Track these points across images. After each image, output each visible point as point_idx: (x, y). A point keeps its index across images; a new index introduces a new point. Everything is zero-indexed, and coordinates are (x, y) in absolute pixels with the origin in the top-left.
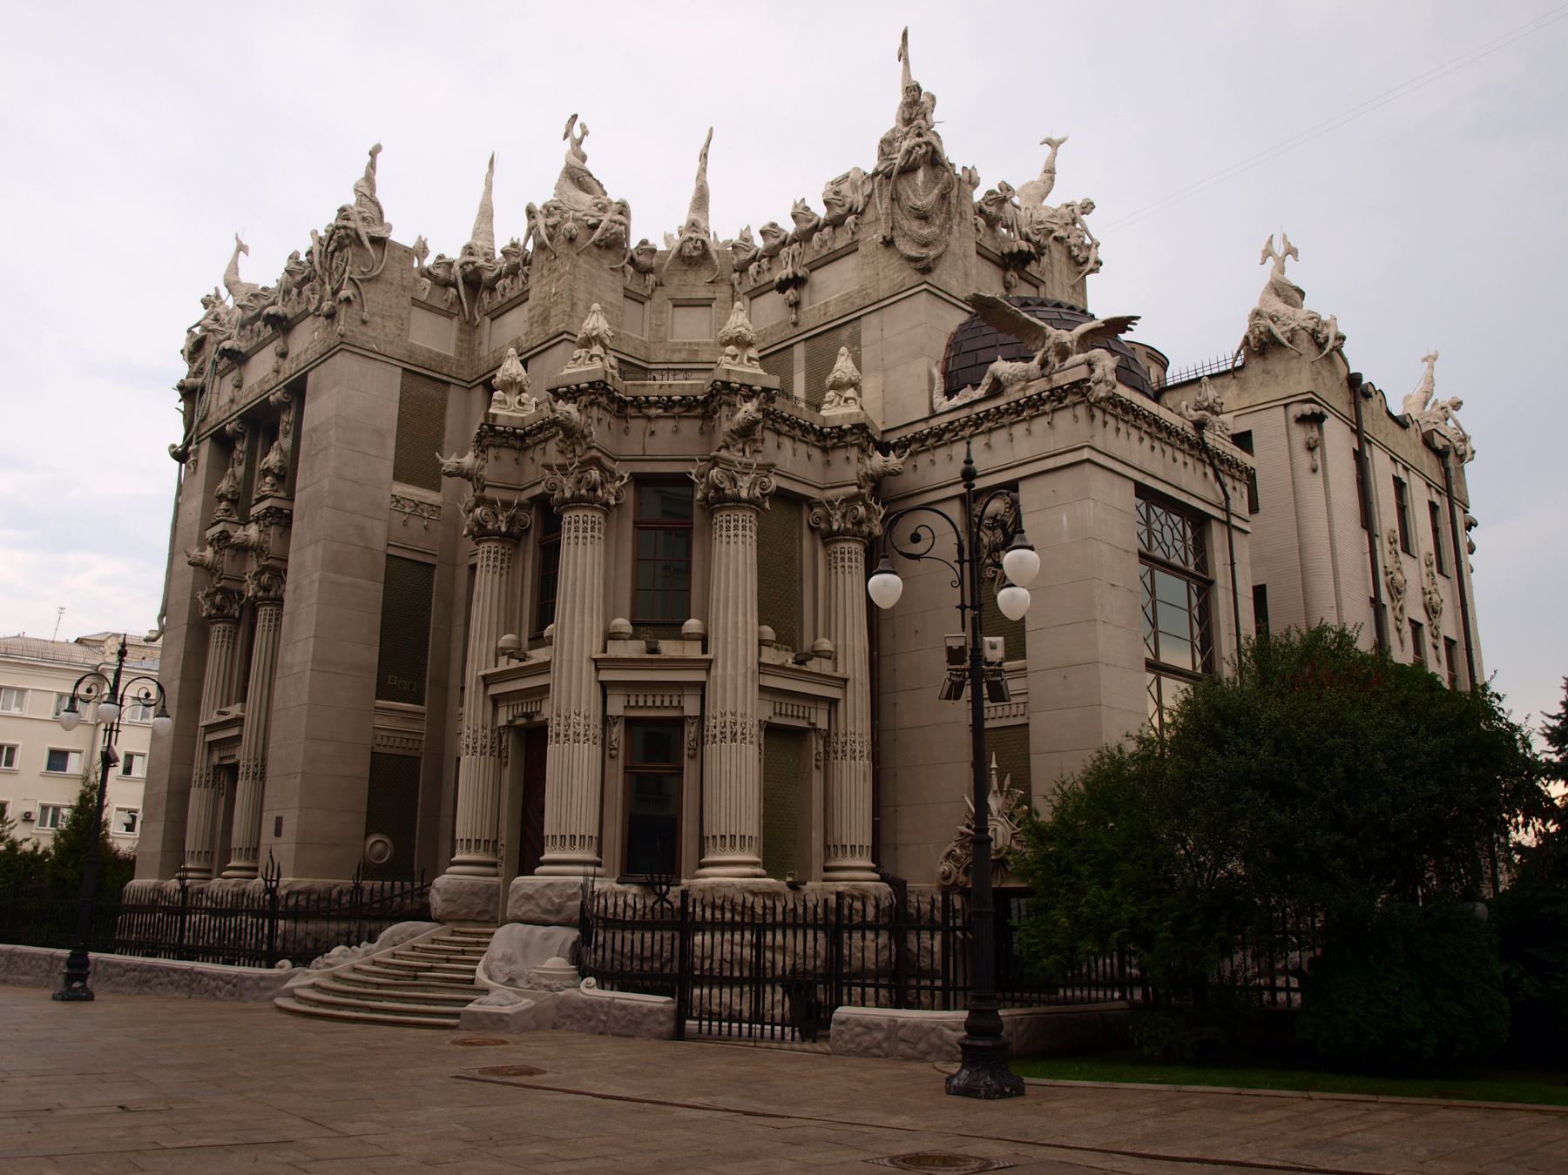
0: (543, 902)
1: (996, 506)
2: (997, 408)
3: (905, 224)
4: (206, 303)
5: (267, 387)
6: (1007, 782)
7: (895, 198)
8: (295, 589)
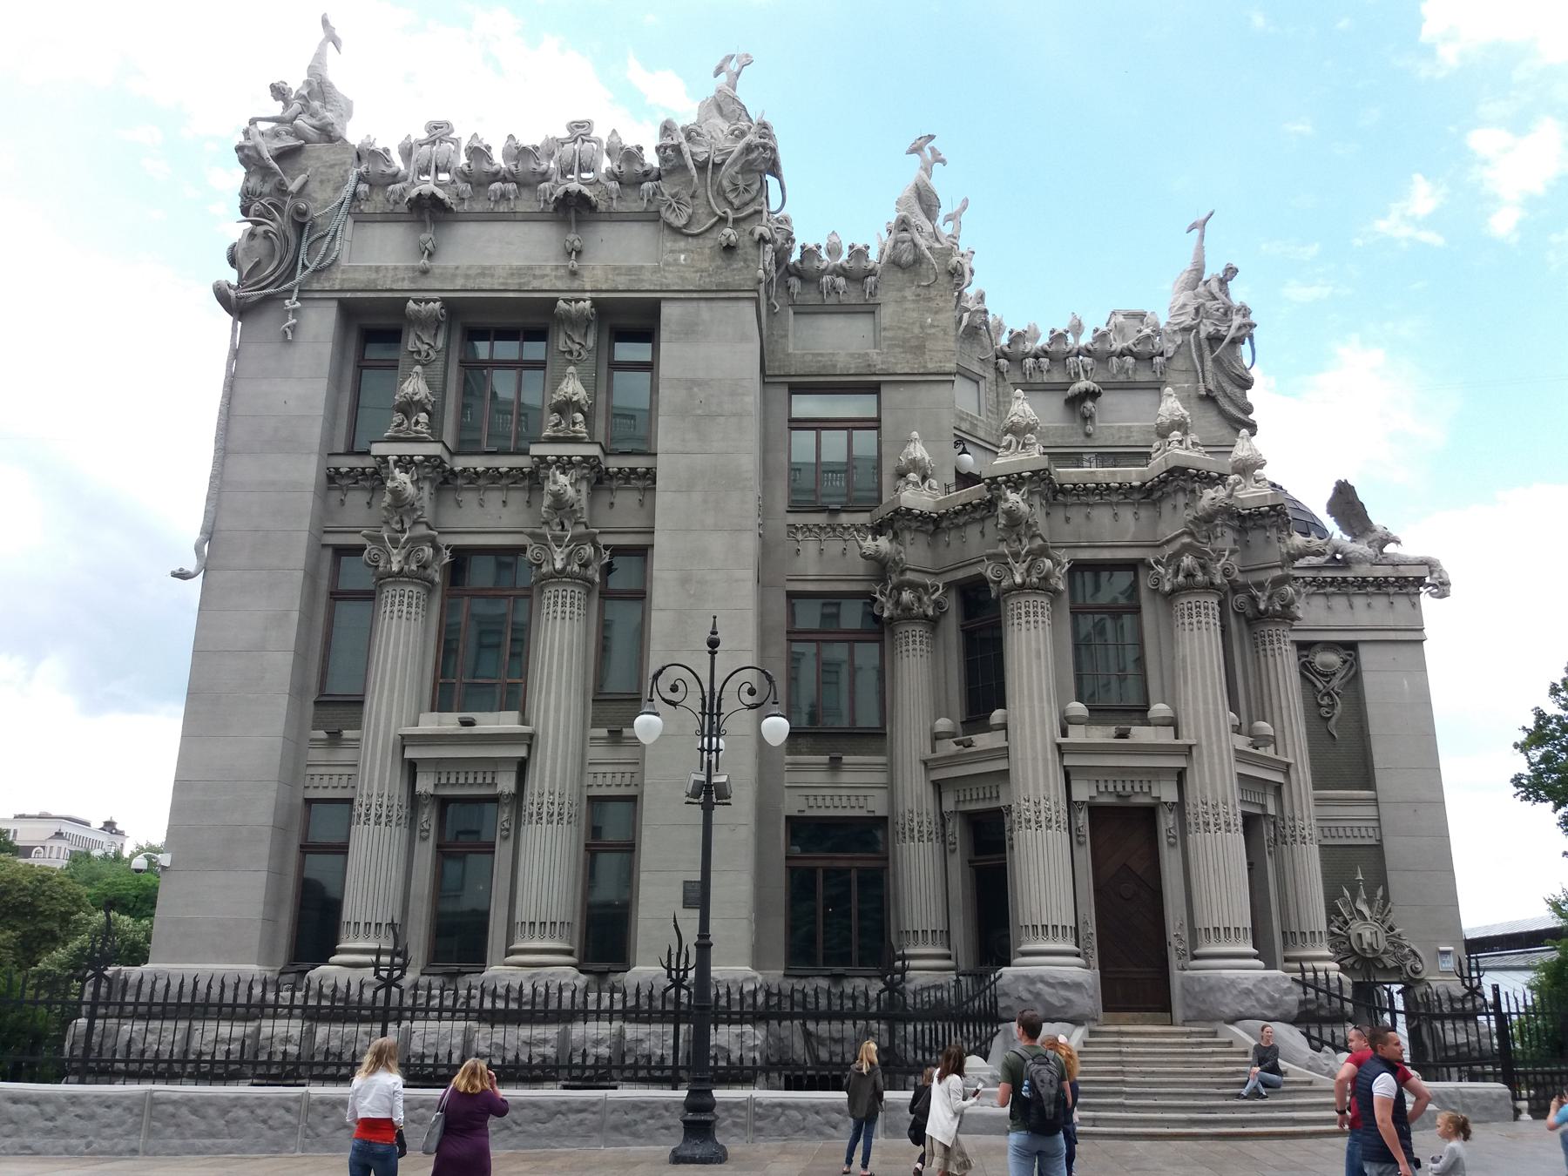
0: (1263, 997)
1: (1332, 659)
2: (1344, 579)
3: (1229, 388)
4: (279, 92)
5: (536, 284)
6: (1380, 892)
7: (1217, 360)
8: (685, 581)
